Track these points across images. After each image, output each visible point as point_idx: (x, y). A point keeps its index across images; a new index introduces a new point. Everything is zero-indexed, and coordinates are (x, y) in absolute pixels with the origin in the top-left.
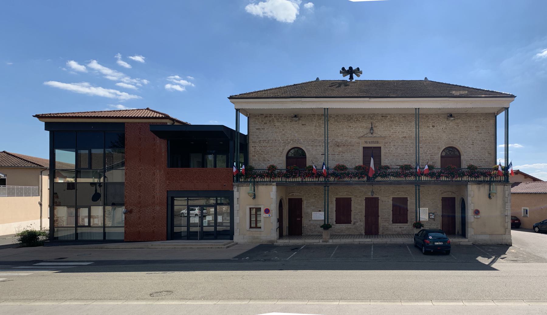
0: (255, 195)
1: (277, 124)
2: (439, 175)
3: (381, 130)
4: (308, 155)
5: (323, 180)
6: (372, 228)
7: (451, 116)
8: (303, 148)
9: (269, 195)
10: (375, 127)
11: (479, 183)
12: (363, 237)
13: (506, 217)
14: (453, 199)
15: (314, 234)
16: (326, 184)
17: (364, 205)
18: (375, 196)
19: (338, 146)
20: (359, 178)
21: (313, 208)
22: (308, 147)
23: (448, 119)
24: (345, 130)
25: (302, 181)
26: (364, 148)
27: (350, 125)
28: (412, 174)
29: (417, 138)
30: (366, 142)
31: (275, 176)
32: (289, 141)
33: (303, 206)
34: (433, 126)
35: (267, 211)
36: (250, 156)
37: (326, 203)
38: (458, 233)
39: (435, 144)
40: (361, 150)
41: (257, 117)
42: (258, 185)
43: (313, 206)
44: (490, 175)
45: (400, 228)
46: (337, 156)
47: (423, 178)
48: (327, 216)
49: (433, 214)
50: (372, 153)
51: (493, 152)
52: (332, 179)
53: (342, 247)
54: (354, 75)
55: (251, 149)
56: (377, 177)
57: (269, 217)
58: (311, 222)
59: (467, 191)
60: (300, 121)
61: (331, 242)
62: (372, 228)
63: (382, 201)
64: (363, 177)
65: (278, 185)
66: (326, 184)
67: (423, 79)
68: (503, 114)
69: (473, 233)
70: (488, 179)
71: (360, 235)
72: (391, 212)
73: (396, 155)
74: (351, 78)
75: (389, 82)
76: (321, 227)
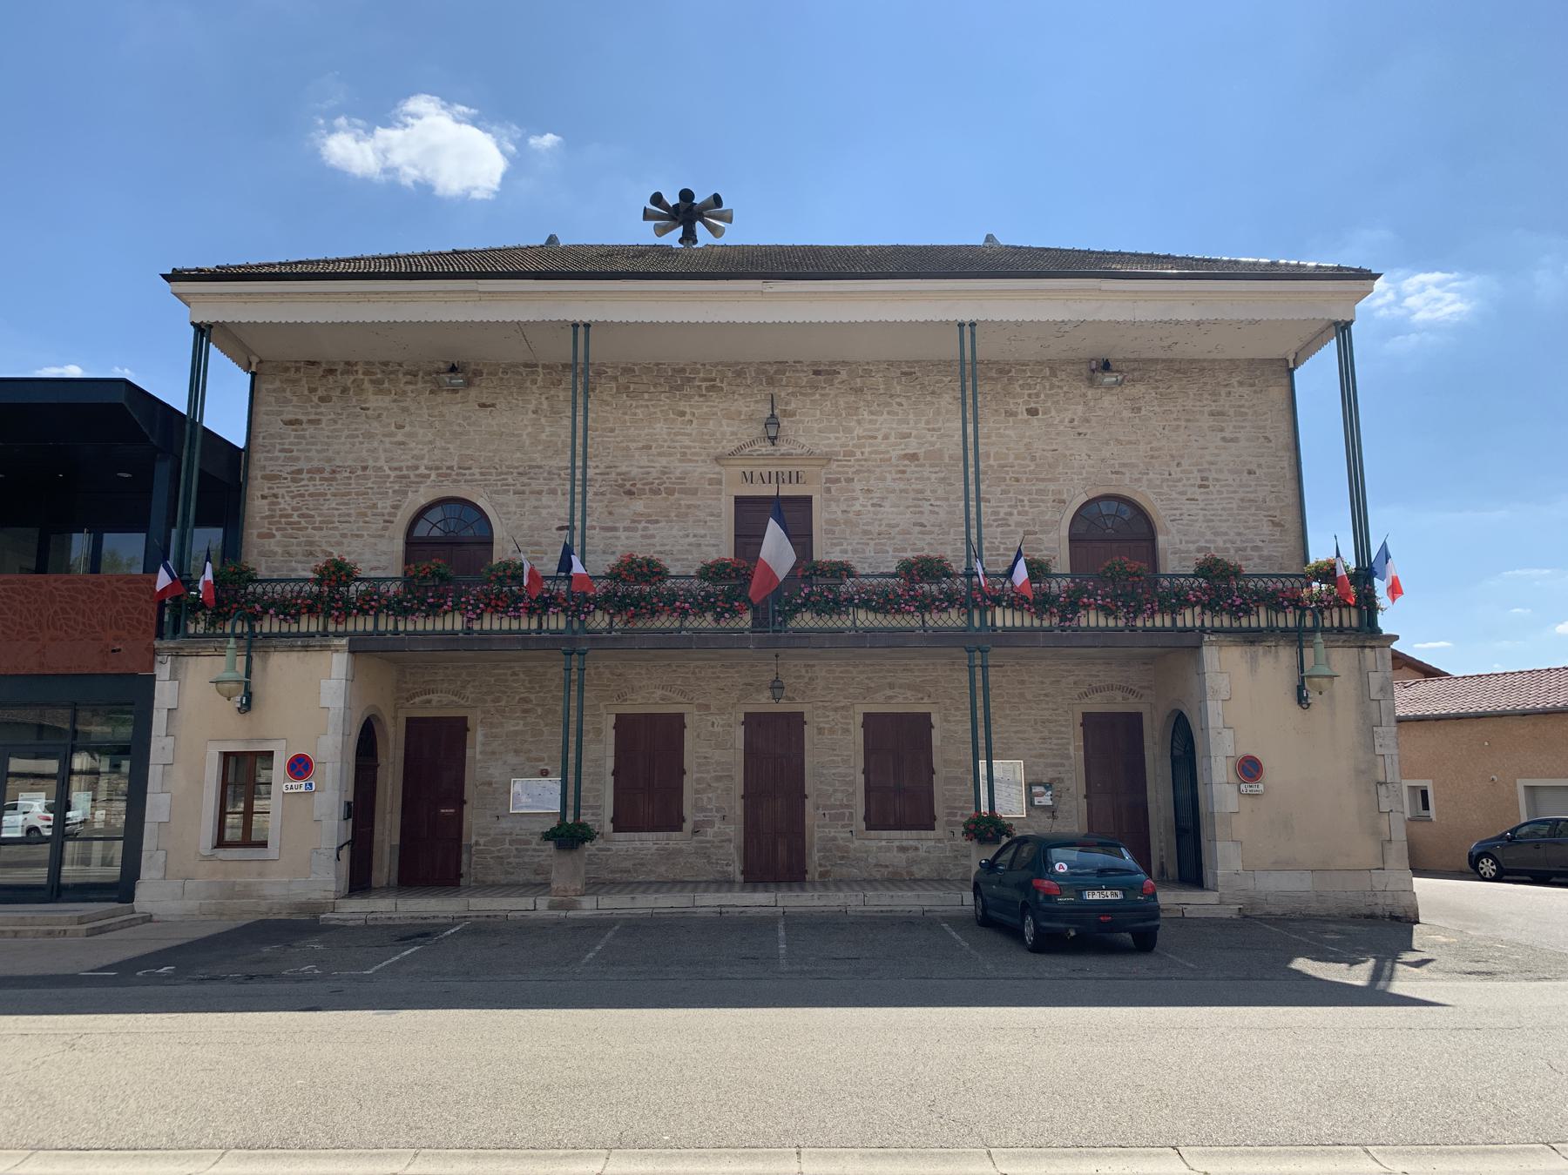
0: (249, 695)
1: (375, 401)
2: (1073, 604)
3: (815, 427)
4: (499, 532)
5: (562, 625)
6: (775, 852)
7: (1106, 366)
9: (314, 697)
10: (785, 413)
11: (1252, 637)
12: (737, 887)
13: (1382, 790)
14: (1133, 722)
15: (513, 878)
16: (571, 647)
17: (740, 744)
18: (783, 707)
19: (630, 493)
20: (719, 617)
21: (512, 759)
23: (1091, 382)
24: (660, 428)
25: (469, 631)
26: (739, 501)
27: (682, 405)
28: (951, 600)
29: (971, 453)
30: (748, 478)
31: (346, 609)
32: (422, 470)
33: (469, 752)
35: (300, 767)
36: (251, 535)
37: (573, 739)
38: (1162, 872)
39: (1041, 486)
40: (727, 509)
41: (292, 374)
42: (266, 651)
43: (516, 752)
44: (1298, 604)
45: (902, 849)
46: (622, 534)
47: (1003, 618)
48: (572, 794)
49: (1048, 786)
51: (1290, 518)
52: (599, 620)
53: (635, 927)
54: (698, 224)
55: (257, 506)
56: (796, 610)
57: (309, 792)
58: (505, 824)
59: (1201, 674)
60: (473, 392)
61: (588, 906)
62: (775, 852)
63: (820, 731)
64: (735, 613)
65: (359, 647)
66: (571, 647)
67: (980, 241)
68: (1330, 350)
69: (1238, 865)
70: (1289, 619)
71: (724, 883)
72: (861, 779)
73: (875, 529)
74: (689, 236)
75: (845, 248)
76: (547, 836)
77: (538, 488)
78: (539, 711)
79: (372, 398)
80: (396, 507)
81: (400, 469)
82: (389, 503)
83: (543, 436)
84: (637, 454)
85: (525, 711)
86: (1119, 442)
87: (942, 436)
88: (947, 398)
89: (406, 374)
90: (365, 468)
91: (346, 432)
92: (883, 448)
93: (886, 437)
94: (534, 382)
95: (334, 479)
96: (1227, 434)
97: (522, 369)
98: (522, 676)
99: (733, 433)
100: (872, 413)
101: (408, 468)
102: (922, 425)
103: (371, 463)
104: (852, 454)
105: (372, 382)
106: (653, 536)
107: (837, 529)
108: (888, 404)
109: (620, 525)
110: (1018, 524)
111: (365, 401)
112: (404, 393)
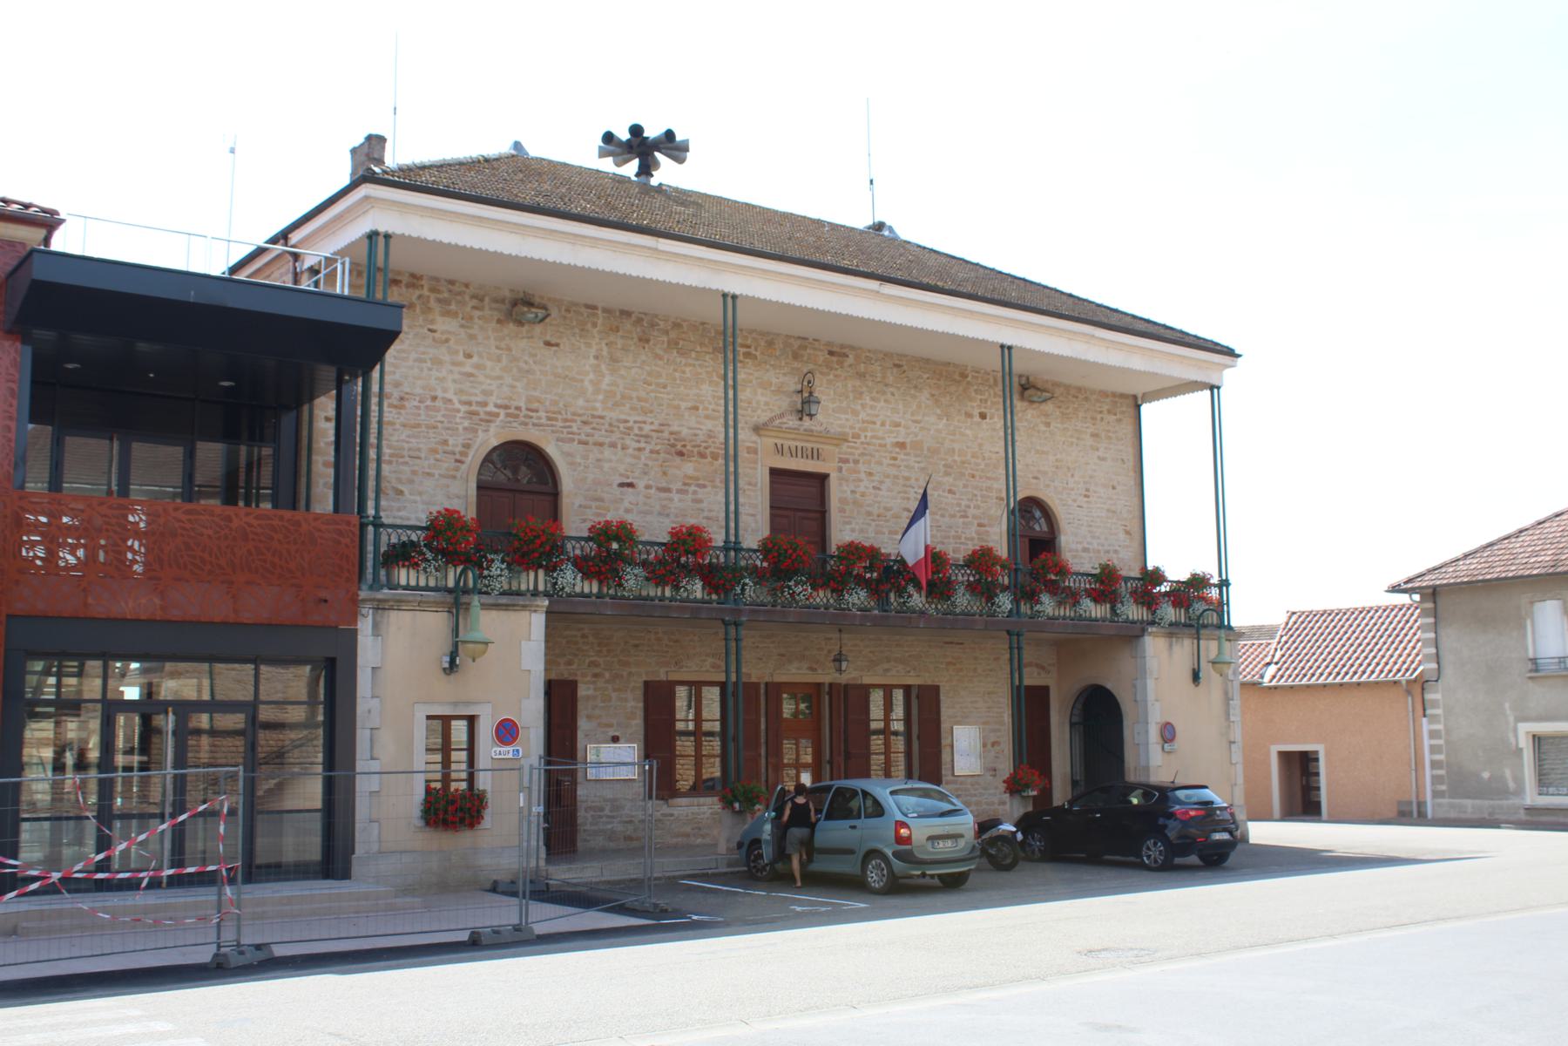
1: (444, 325)
8: (551, 450)
19: (681, 454)
22: (566, 447)
26: (775, 473)
30: (779, 450)
32: (491, 408)
34: (983, 416)
39: (989, 483)
46: (676, 497)
50: (801, 496)
51: (1136, 530)
73: (875, 511)
77: (601, 440)
78: (607, 675)
79: (439, 319)
80: (467, 446)
81: (469, 403)
82: (460, 440)
83: (604, 386)
84: (686, 414)
85: (595, 675)
86: (1037, 452)
87: (922, 429)
88: (926, 394)
89: (473, 297)
90: (434, 398)
91: (414, 355)
92: (880, 434)
93: (883, 424)
94: (595, 325)
95: (402, 407)
96: (1100, 454)
97: (583, 310)
98: (591, 639)
99: (767, 404)
100: (873, 399)
101: (478, 403)
102: (908, 416)
103: (439, 394)
104: (856, 436)
105: (439, 301)
106: (701, 501)
107: (847, 508)
108: (884, 393)
109: (674, 487)
110: (974, 517)
111: (432, 322)
112: (471, 318)
